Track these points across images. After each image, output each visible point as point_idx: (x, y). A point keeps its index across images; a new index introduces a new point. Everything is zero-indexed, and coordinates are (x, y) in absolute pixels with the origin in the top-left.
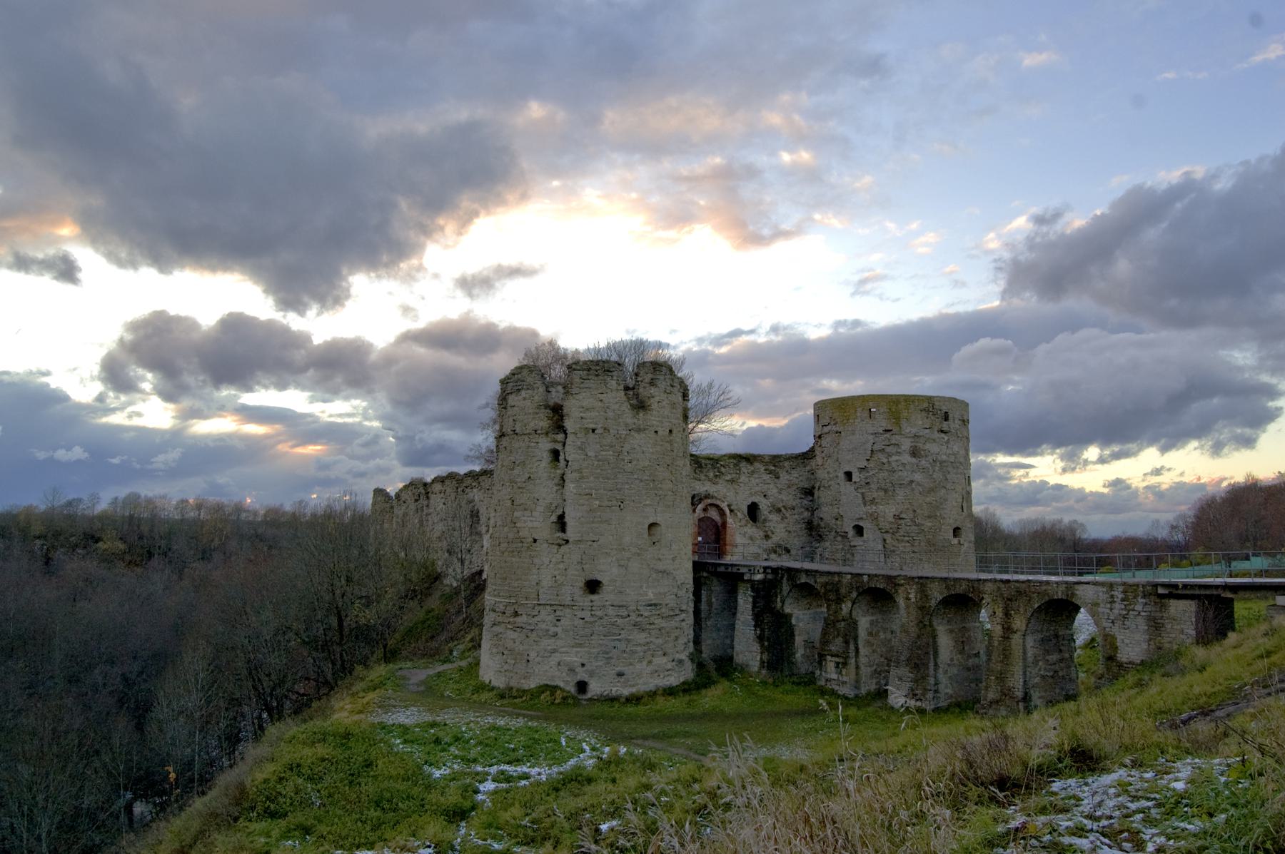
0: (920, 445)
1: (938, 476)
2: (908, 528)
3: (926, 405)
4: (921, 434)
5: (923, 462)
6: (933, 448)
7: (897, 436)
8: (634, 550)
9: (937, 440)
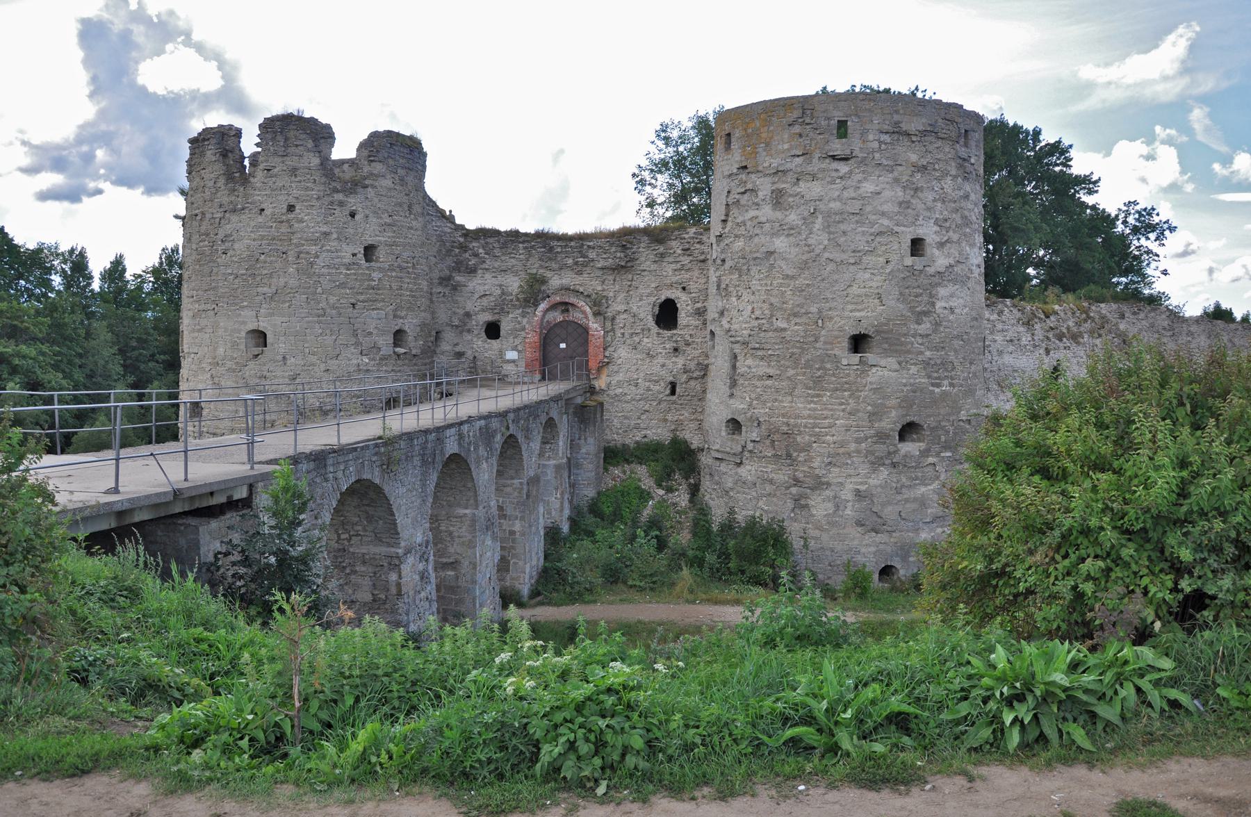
2: (762, 334)
3: (797, 113)
4: (788, 166)
6: (812, 189)
7: (753, 176)
8: (229, 364)
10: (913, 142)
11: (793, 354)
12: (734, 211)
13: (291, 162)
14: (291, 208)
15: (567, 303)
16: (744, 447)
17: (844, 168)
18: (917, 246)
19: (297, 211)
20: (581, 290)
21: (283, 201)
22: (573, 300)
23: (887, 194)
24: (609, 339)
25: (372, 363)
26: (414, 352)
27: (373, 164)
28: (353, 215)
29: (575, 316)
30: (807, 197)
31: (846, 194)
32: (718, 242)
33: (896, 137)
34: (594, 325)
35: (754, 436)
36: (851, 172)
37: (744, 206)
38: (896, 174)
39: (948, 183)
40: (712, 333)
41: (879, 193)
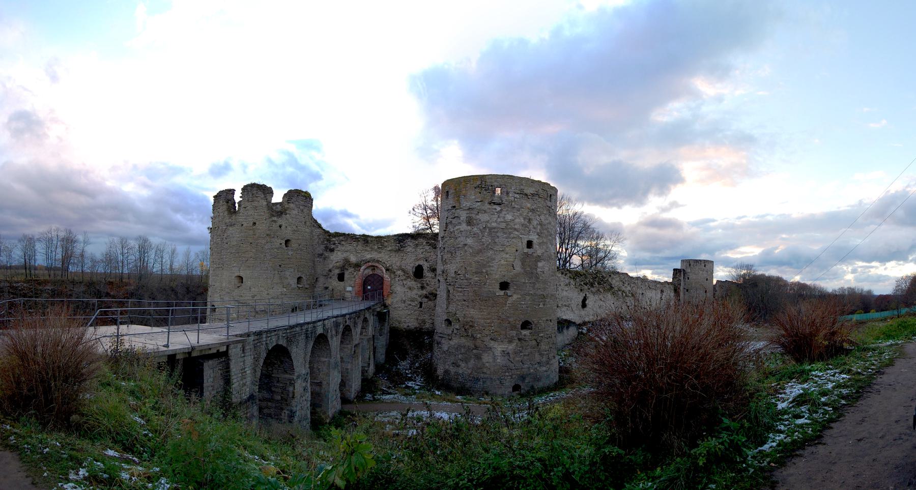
0: (473, 216)
1: (487, 239)
5: (475, 229)
6: (484, 217)
8: (227, 290)
9: (488, 211)
10: (529, 198)
11: (475, 290)
12: (450, 226)
13: (255, 204)
14: (254, 224)
15: (374, 266)
16: (453, 332)
17: (498, 208)
18: (530, 244)
19: (257, 225)
20: (381, 260)
21: (251, 220)
22: (376, 264)
23: (517, 220)
24: (393, 282)
25: (288, 291)
26: (307, 286)
27: (289, 204)
28: (280, 226)
29: (377, 272)
30: (482, 220)
31: (499, 220)
32: (442, 240)
33: (521, 195)
34: (386, 276)
35: (457, 327)
36: (501, 210)
37: (454, 224)
38: (521, 212)
39: (542, 217)
40: (439, 280)
41: (513, 220)
